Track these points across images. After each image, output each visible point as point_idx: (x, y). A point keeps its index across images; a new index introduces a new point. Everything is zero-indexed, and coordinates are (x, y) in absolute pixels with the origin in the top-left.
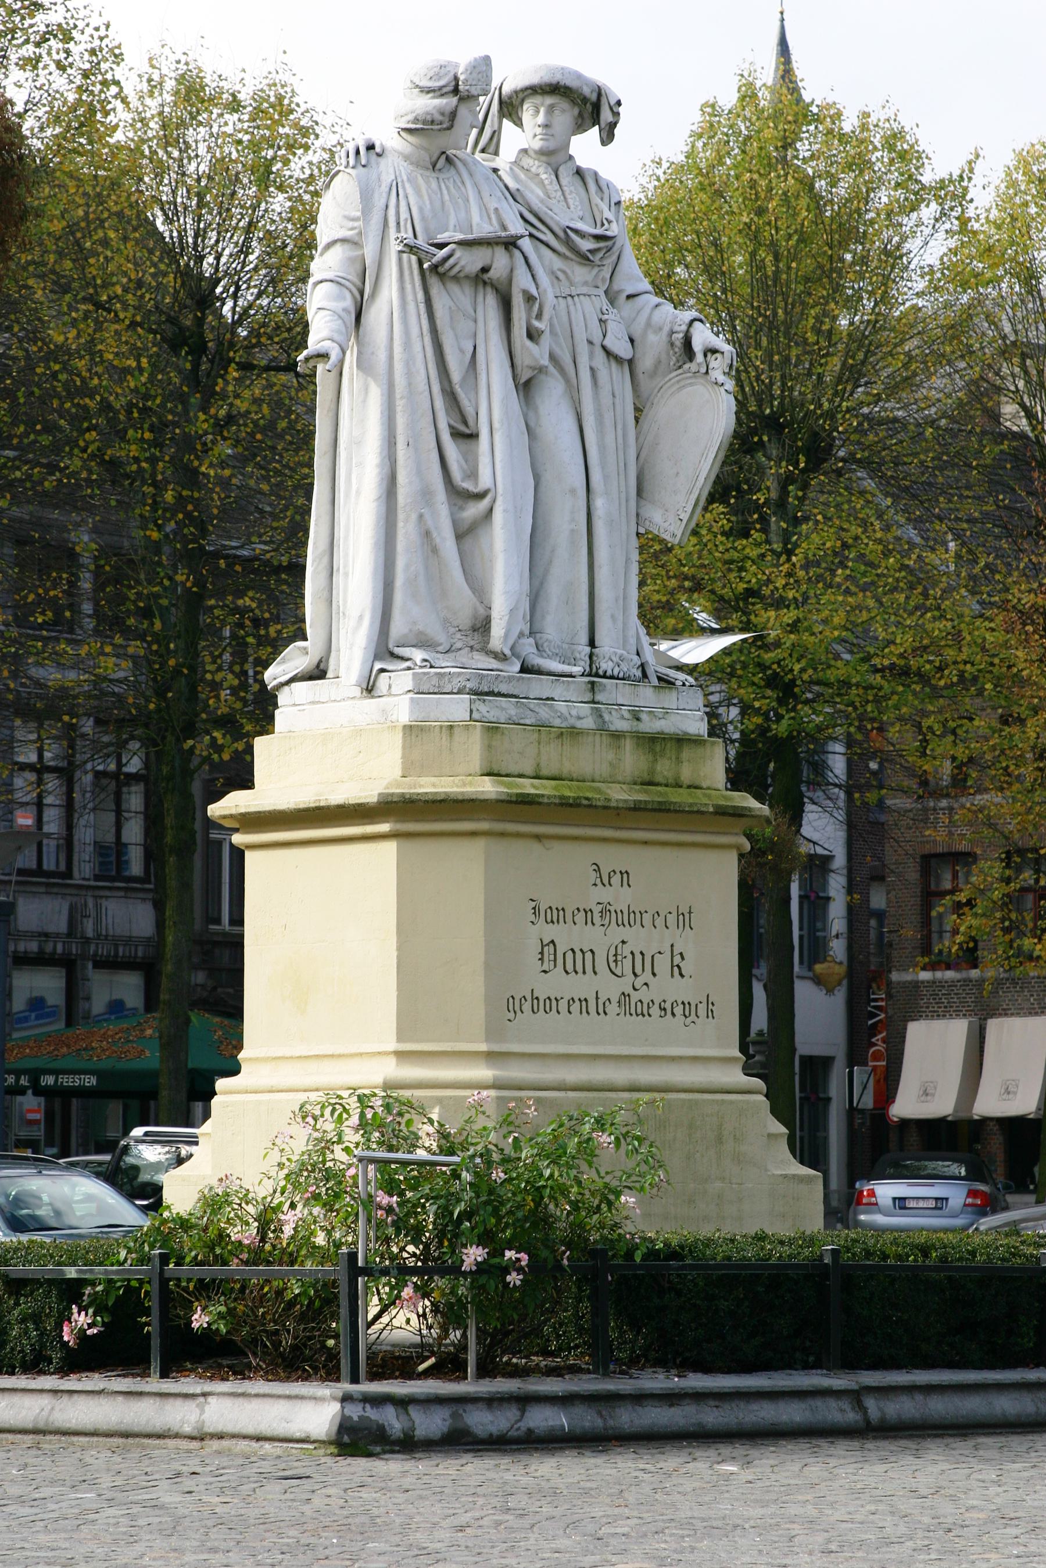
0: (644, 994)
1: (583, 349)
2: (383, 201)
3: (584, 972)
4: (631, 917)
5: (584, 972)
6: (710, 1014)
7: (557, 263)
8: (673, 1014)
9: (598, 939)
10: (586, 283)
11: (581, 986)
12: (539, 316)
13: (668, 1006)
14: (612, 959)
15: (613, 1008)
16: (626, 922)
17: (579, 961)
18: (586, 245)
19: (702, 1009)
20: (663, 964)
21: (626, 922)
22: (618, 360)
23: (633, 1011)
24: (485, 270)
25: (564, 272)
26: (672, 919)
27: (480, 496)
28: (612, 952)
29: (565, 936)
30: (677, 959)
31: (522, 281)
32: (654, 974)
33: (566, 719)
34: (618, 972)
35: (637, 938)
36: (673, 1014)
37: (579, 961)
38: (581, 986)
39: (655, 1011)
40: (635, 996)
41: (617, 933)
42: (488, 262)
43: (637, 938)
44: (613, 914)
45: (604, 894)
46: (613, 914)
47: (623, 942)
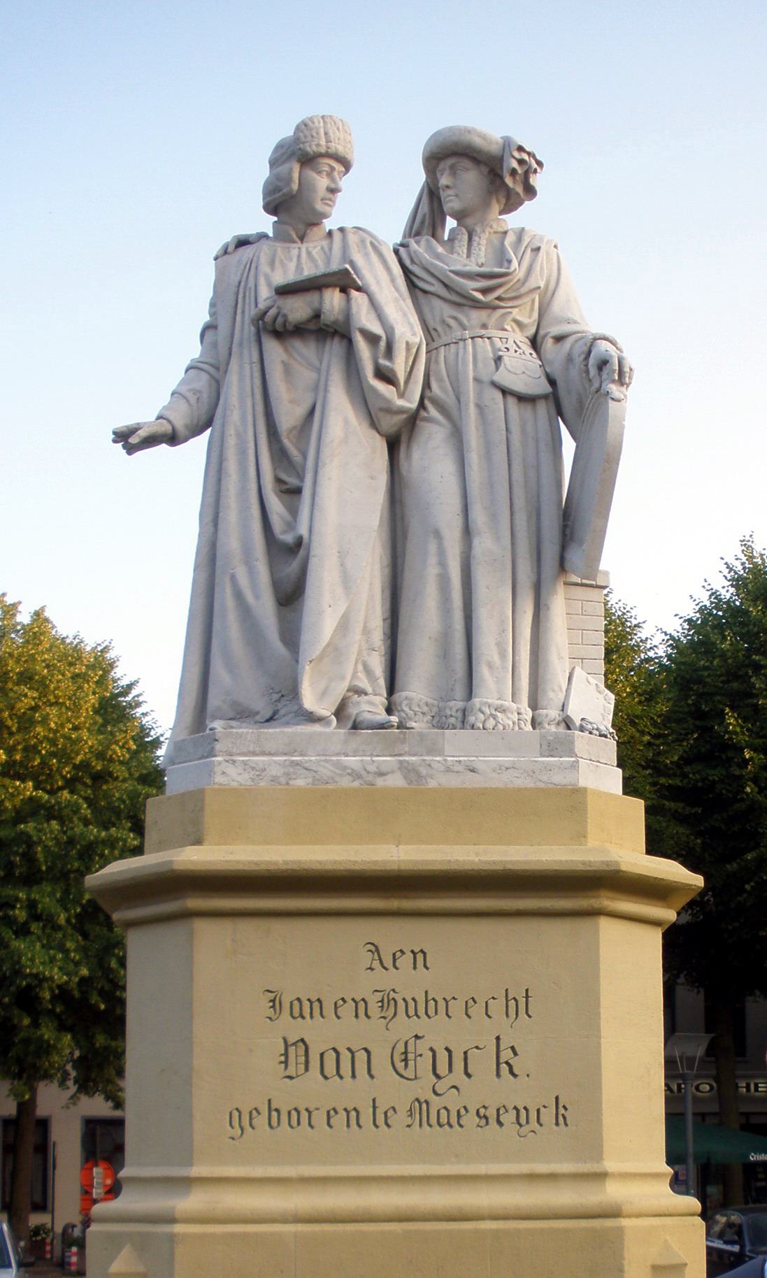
0: (453, 1101)
1: (470, 388)
2: (237, 279)
3: (354, 1076)
4: (430, 1006)
5: (354, 1076)
6: (560, 1118)
7: (448, 310)
8: (500, 1123)
9: (379, 1036)
11: (354, 1092)
13: (492, 1113)
14: (397, 1058)
15: (399, 1120)
16: (421, 1011)
17: (338, 1063)
19: (548, 1115)
20: (483, 1063)
21: (421, 1011)
23: (433, 1120)
24: (317, 315)
25: (455, 318)
26: (497, 1007)
27: (299, 542)
28: (400, 1048)
30: (506, 1055)
31: (365, 318)
32: (469, 1075)
33: (359, 776)
34: (410, 1073)
35: (439, 1033)
36: (500, 1123)
38: (354, 1092)
39: (470, 1120)
40: (436, 1103)
41: (404, 1027)
42: (316, 304)
43: (439, 1033)
44: (401, 1004)
46: (401, 1004)
47: (417, 1037)
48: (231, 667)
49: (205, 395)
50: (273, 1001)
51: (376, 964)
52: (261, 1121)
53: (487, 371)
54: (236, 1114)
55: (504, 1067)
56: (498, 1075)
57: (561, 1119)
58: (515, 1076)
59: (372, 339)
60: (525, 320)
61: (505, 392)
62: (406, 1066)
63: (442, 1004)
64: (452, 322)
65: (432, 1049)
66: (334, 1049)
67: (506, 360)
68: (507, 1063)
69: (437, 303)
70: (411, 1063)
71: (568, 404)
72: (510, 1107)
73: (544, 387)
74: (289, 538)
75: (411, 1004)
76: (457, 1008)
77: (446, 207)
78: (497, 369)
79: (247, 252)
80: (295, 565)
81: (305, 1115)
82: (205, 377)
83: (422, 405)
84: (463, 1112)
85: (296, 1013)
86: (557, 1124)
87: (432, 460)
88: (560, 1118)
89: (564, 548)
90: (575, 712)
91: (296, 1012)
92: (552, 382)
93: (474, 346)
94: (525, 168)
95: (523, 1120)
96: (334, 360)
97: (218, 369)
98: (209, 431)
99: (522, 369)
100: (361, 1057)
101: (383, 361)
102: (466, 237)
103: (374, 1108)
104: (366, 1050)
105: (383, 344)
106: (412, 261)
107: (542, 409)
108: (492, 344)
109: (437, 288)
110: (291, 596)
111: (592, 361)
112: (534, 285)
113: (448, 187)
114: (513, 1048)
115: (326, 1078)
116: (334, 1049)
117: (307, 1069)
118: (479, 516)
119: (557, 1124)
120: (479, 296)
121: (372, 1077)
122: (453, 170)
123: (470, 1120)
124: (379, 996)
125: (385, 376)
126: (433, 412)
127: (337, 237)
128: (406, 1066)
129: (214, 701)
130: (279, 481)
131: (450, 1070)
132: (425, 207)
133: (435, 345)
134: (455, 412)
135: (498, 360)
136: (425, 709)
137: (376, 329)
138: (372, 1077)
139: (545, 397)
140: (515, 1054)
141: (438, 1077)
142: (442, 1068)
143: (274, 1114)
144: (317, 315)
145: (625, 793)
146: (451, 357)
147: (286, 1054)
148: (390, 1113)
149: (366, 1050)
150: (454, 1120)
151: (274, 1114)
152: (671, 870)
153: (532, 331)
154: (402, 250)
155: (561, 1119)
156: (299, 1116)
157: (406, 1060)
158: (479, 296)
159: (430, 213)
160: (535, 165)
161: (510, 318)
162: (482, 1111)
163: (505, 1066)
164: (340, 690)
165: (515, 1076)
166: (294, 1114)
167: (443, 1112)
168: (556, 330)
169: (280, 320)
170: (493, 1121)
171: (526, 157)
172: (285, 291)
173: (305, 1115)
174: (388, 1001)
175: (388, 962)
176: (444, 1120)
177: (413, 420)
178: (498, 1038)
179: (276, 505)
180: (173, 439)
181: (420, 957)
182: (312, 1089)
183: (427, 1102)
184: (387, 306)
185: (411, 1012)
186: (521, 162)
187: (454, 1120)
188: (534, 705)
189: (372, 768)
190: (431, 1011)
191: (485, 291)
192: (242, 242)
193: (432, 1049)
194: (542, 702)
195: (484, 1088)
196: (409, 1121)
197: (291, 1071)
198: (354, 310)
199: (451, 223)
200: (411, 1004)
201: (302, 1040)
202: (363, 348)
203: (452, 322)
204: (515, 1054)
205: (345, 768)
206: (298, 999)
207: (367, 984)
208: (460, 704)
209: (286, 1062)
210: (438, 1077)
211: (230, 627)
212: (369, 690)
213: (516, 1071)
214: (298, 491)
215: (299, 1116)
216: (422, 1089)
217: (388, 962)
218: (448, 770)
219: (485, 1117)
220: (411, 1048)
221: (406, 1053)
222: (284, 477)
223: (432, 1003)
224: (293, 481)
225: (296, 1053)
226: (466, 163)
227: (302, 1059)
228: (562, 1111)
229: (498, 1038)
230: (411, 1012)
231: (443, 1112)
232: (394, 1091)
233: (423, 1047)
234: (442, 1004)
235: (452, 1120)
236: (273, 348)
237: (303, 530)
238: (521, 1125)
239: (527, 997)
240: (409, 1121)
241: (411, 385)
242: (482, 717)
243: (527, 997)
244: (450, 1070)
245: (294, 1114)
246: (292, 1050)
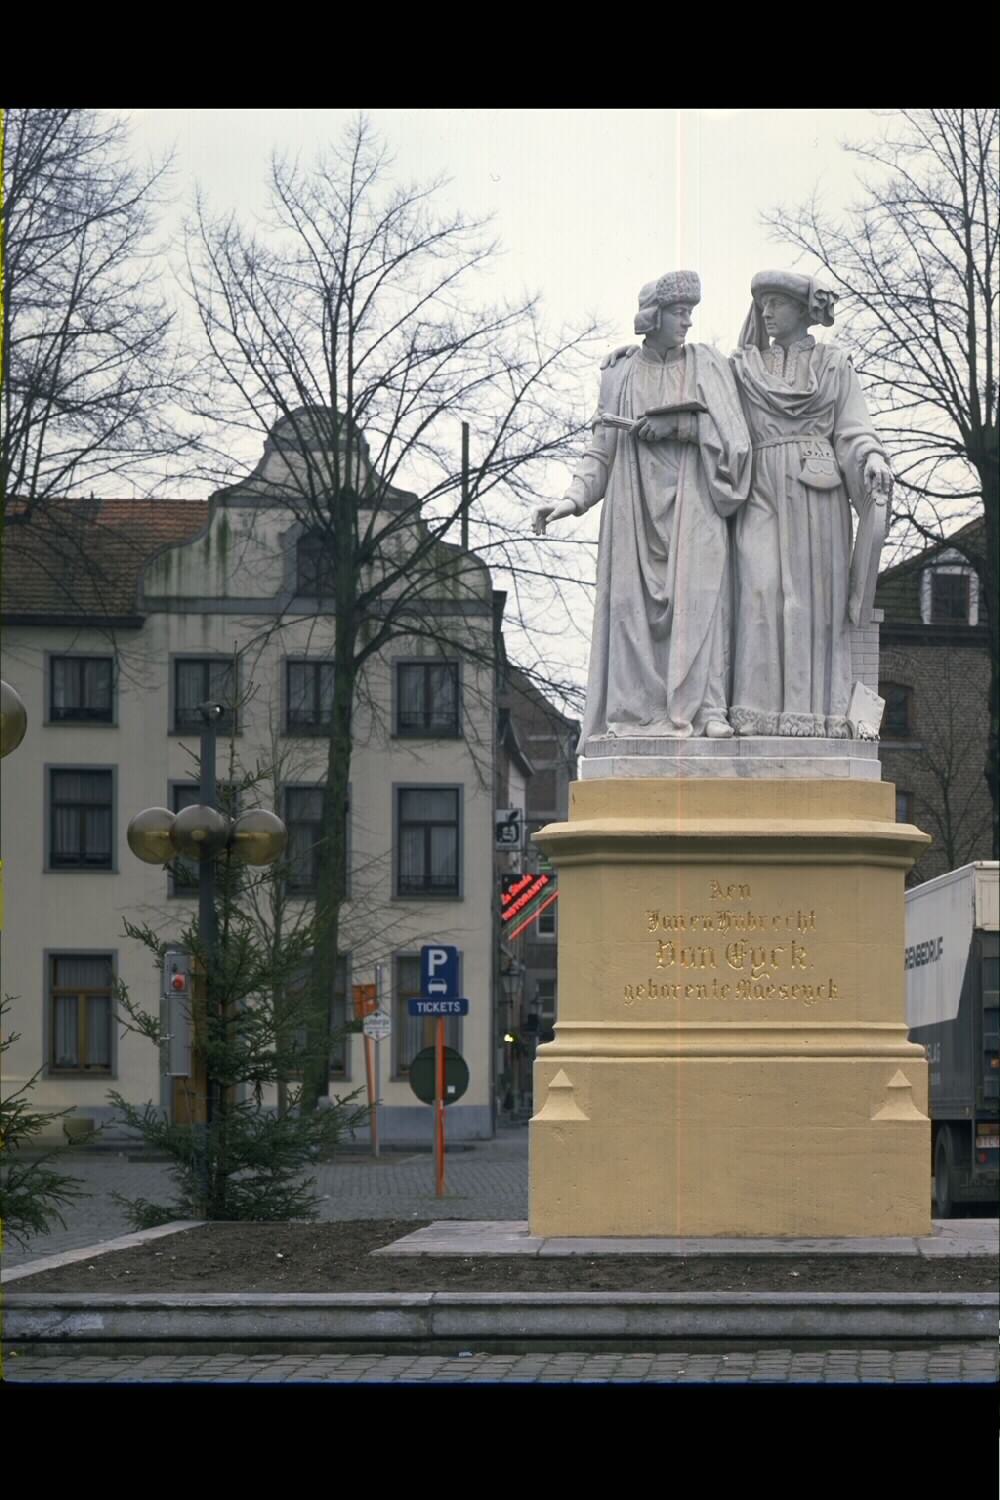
7: (769, 420)
10: (793, 433)
22: (823, 492)
31: (710, 438)
42: (675, 425)
48: (620, 685)
49: (598, 479)
53: (796, 472)
59: (714, 451)
60: (824, 425)
61: (807, 487)
64: (772, 430)
67: (808, 461)
69: (762, 414)
71: (854, 490)
73: (836, 480)
74: (659, 597)
77: (769, 331)
78: (802, 468)
79: (625, 363)
80: (662, 619)
82: (597, 463)
83: (750, 495)
87: (759, 542)
89: (849, 598)
90: (854, 718)
92: (842, 474)
93: (787, 450)
96: (688, 462)
97: (606, 457)
98: (602, 501)
99: (822, 470)
101: (723, 468)
102: (782, 356)
105: (721, 455)
106: (745, 375)
107: (835, 499)
108: (799, 447)
109: (760, 402)
110: (660, 635)
111: (866, 472)
112: (830, 400)
113: (768, 317)
118: (787, 580)
120: (789, 412)
122: (773, 303)
125: (723, 477)
126: (758, 500)
127: (689, 356)
129: (611, 709)
130: (651, 552)
132: (753, 324)
133: (760, 445)
134: (774, 502)
135: (803, 461)
137: (718, 444)
139: (837, 488)
144: (676, 431)
145: (883, 779)
146: (771, 456)
152: (910, 831)
153: (831, 431)
154: (737, 361)
158: (789, 412)
159: (757, 333)
160: (832, 300)
161: (812, 425)
164: (697, 704)
168: (845, 433)
169: (649, 434)
172: (651, 415)
177: (745, 506)
180: (578, 511)
181: (745, 889)
184: (728, 427)
186: (821, 301)
188: (827, 712)
191: (793, 408)
192: (621, 355)
194: (833, 710)
198: (701, 431)
199: (772, 340)
202: (705, 452)
203: (772, 430)
208: (776, 714)
211: (619, 658)
214: (664, 560)
217: (725, 891)
222: (655, 549)
224: (661, 553)
226: (781, 299)
236: (647, 458)
237: (668, 595)
241: (743, 483)
242: (788, 725)
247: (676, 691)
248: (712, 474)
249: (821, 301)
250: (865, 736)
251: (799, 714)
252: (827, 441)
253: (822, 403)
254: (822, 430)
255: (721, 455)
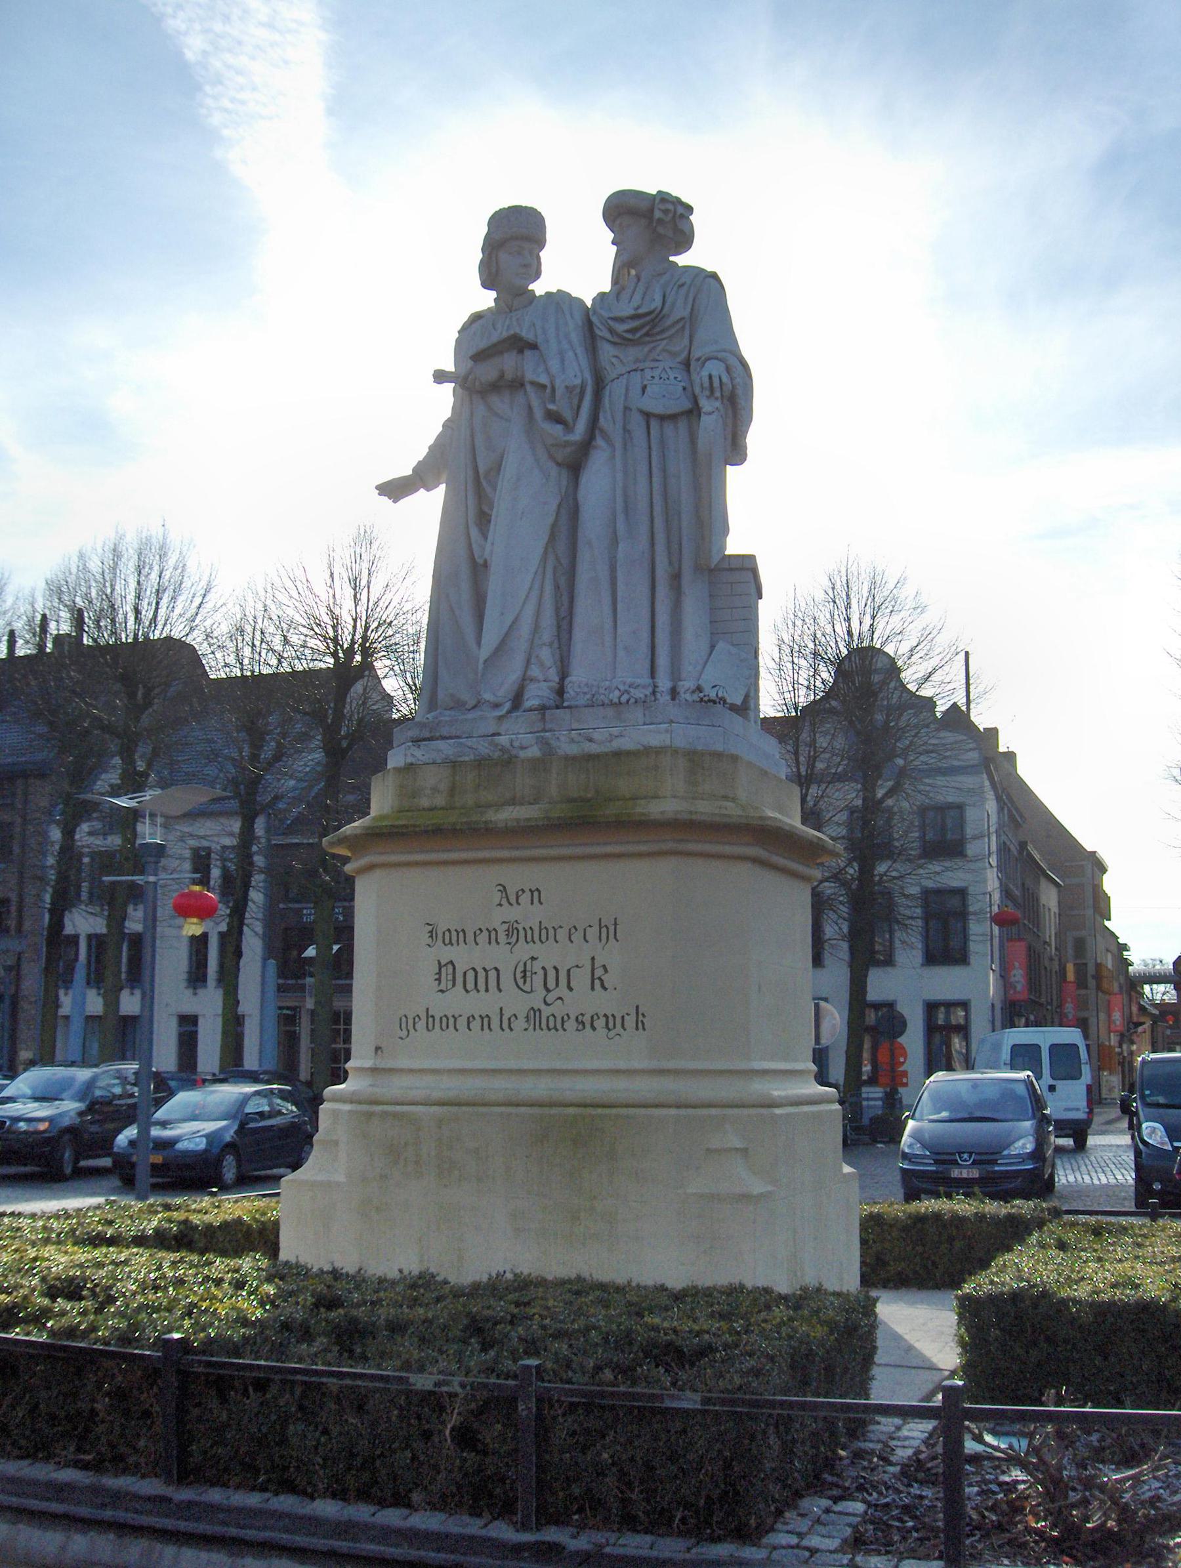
0: (557, 1009)
3: (487, 990)
4: (544, 933)
5: (487, 990)
6: (639, 1025)
8: (594, 1029)
9: (504, 957)
12: (553, 399)
14: (519, 975)
15: (519, 1024)
18: (621, 328)
19: (630, 1021)
20: (581, 979)
23: (544, 1025)
26: (592, 933)
28: (520, 968)
29: (463, 956)
30: (599, 972)
32: (571, 989)
34: (527, 988)
35: (549, 955)
36: (594, 1029)
37: (482, 979)
39: (571, 1025)
40: (547, 1012)
41: (523, 951)
43: (549, 955)
44: (522, 933)
45: (512, 913)
46: (522, 933)
47: (533, 959)
50: (431, 932)
51: (504, 902)
52: (421, 1025)
54: (404, 1019)
55: (597, 982)
56: (593, 988)
57: (640, 1025)
58: (605, 989)
62: (525, 982)
63: (551, 932)
64: (614, 360)
65: (543, 968)
66: (474, 969)
68: (600, 978)
70: (528, 980)
72: (601, 1014)
75: (529, 932)
76: (562, 934)
81: (451, 1021)
84: (566, 1018)
85: (447, 941)
86: (637, 1029)
88: (639, 1025)
91: (447, 941)
94: (671, 215)
95: (611, 1025)
100: (492, 975)
101: (551, 407)
103: (502, 1015)
104: (496, 969)
105: (548, 391)
114: (604, 966)
115: (467, 991)
116: (474, 969)
117: (454, 985)
119: (637, 1029)
120: (629, 336)
121: (500, 990)
123: (571, 1025)
124: (505, 926)
128: (525, 982)
131: (557, 985)
135: (644, 388)
136: (586, 690)
137: (543, 379)
138: (500, 990)
140: (606, 971)
141: (548, 990)
142: (551, 983)
143: (431, 1020)
147: (439, 973)
148: (513, 1019)
149: (496, 969)
150: (559, 1026)
151: (431, 1020)
155: (640, 1025)
156: (448, 1022)
157: (524, 977)
158: (629, 336)
162: (580, 1018)
163: (597, 981)
165: (605, 989)
166: (444, 1019)
167: (551, 1018)
170: (588, 1026)
171: (671, 207)
173: (451, 1021)
174: (512, 930)
175: (513, 899)
176: (551, 1025)
178: (593, 959)
179: (474, 532)
182: (458, 1002)
183: (539, 1010)
185: (529, 939)
187: (559, 1026)
189: (516, 744)
190: (544, 938)
191: (633, 331)
193: (543, 968)
195: (582, 999)
196: (526, 1026)
197: (442, 987)
200: (529, 932)
201: (451, 962)
204: (606, 971)
205: (497, 745)
206: (449, 930)
207: (499, 917)
209: (439, 980)
210: (548, 990)
212: (541, 677)
213: (606, 985)
215: (448, 1022)
216: (536, 1000)
217: (513, 899)
218: (572, 741)
219: (583, 1023)
220: (528, 968)
221: (525, 971)
223: (544, 931)
225: (445, 972)
227: (450, 977)
228: (641, 1018)
229: (593, 959)
230: (529, 939)
231: (551, 1018)
232: (516, 1002)
233: (537, 967)
234: (551, 932)
235: (557, 1024)
238: (609, 1030)
239: (616, 924)
240: (526, 1026)
243: (616, 924)
244: (557, 985)
245: (444, 1019)
246: (443, 969)
247: (485, 661)
248: (539, 414)
249: (666, 212)
250: (706, 699)
251: (629, 680)
252: (682, 367)
253: (669, 322)
254: (674, 355)
255: (548, 391)
